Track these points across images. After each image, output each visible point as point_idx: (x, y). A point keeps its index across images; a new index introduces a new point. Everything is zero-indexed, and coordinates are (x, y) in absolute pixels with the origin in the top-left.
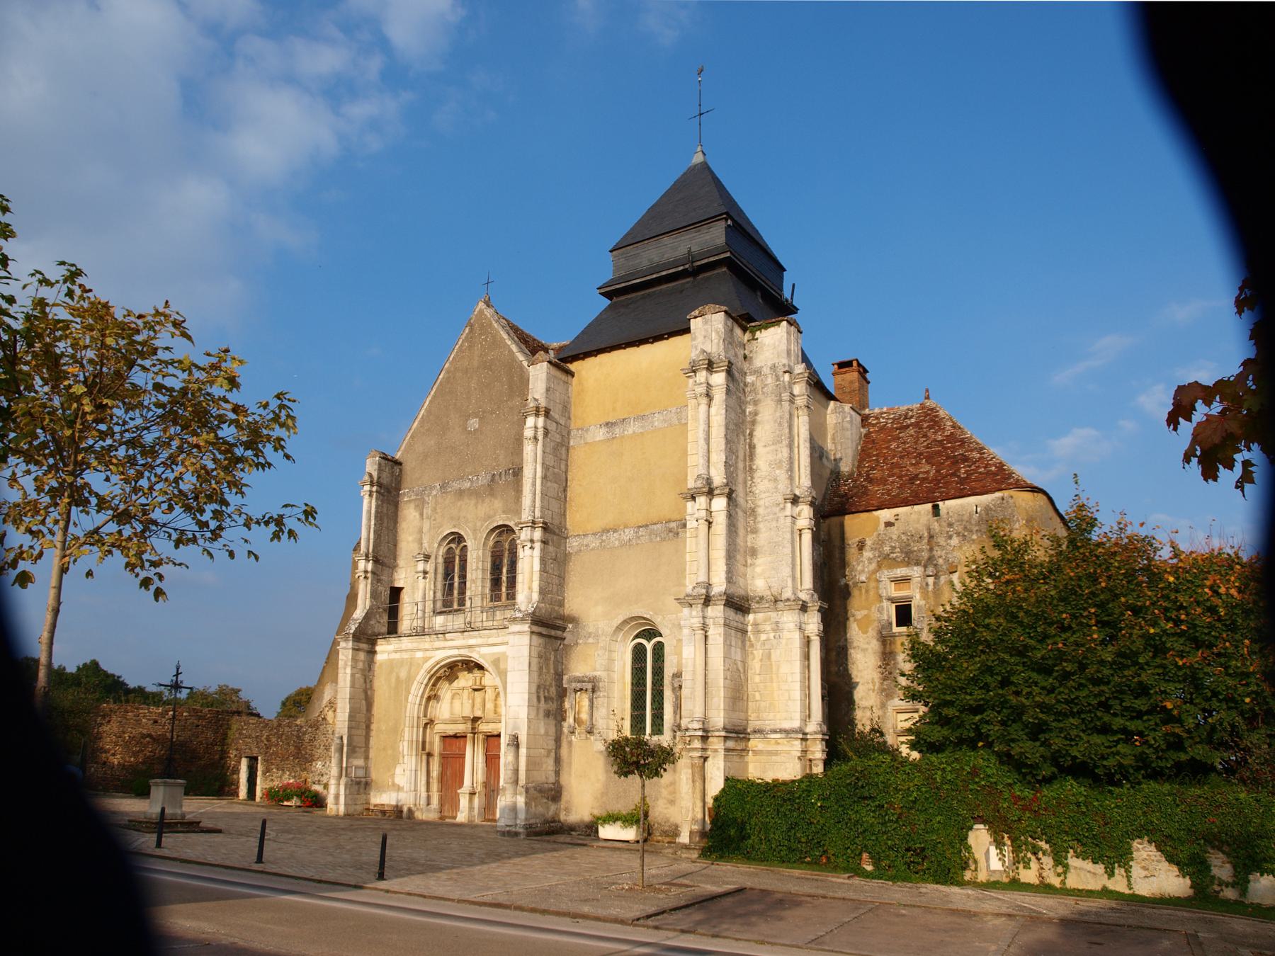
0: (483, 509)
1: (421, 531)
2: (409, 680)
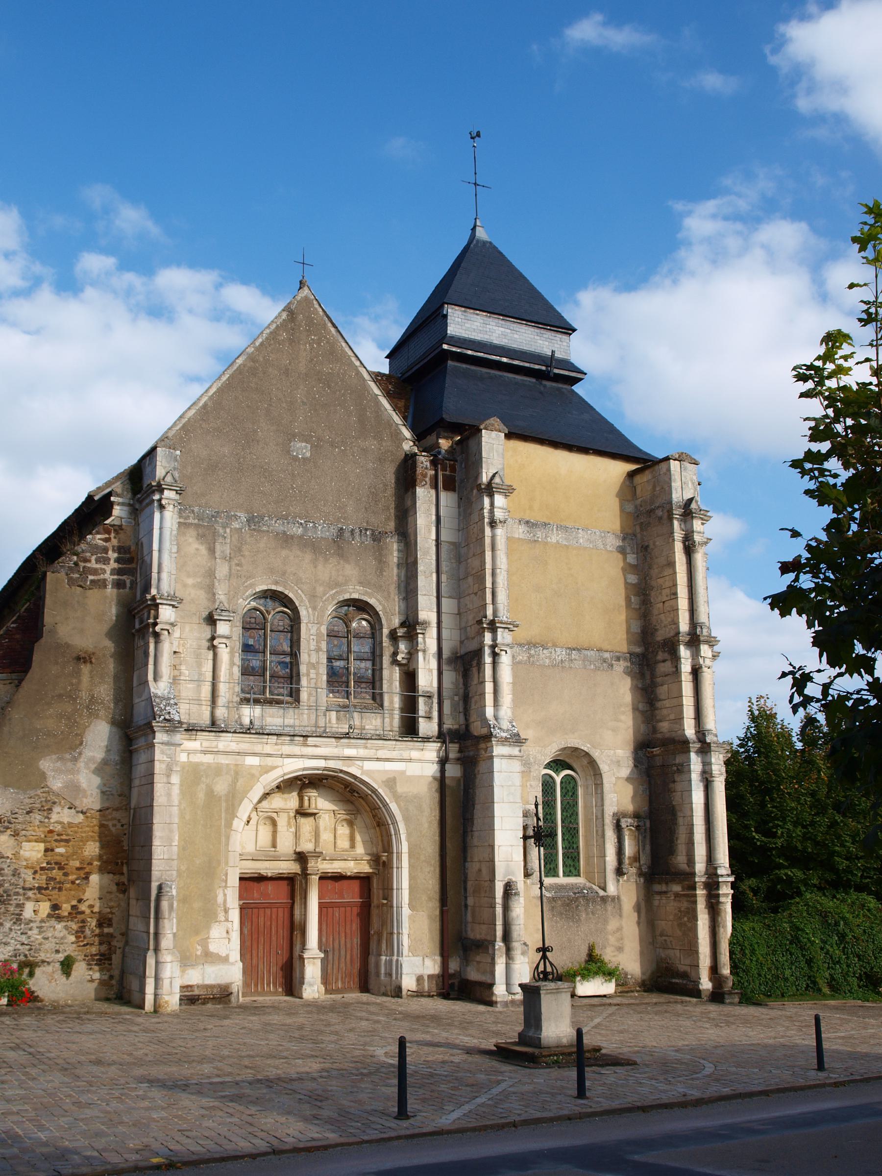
0: (327, 570)
1: (211, 574)
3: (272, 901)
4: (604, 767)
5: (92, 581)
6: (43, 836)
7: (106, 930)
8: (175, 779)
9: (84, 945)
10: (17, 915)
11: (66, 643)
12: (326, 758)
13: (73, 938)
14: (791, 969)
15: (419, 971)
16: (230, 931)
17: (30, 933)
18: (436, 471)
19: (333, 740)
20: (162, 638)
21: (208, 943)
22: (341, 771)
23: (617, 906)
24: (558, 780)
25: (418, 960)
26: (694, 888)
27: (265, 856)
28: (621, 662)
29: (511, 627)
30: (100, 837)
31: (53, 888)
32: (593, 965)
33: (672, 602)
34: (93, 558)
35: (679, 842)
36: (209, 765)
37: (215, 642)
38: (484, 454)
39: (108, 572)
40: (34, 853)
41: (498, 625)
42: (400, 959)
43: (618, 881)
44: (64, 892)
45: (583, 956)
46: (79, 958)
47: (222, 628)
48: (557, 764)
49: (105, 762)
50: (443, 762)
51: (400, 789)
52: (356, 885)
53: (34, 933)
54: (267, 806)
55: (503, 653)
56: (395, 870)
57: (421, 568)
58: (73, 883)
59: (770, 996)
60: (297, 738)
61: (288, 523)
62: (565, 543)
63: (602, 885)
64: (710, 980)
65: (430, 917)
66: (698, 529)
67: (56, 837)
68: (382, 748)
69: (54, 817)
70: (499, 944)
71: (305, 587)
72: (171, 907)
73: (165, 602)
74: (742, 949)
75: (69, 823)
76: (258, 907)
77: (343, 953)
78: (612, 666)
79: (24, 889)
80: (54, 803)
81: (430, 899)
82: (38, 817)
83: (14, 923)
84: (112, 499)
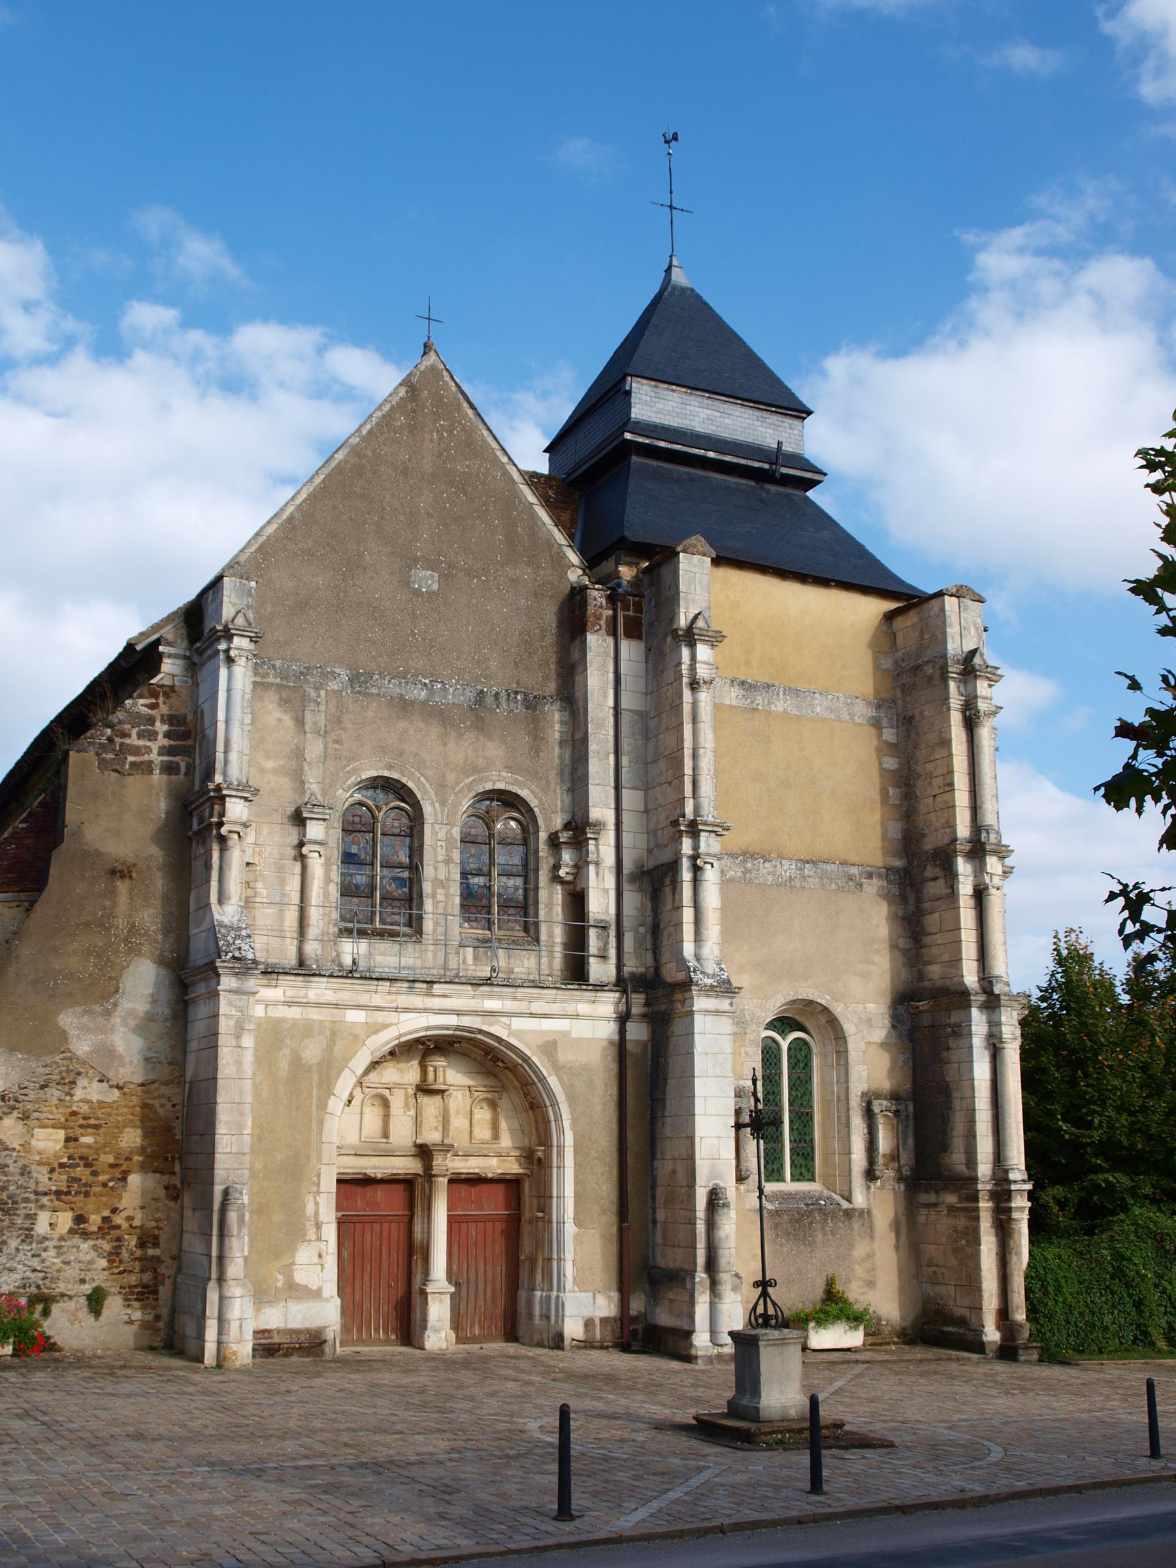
0: (461, 749)
1: (298, 754)
2: (329, 1070)
3: (381, 1212)
4: (849, 1028)
5: (133, 764)
6: (63, 1120)
7: (151, 1252)
8: (248, 1041)
9: (120, 1273)
10: (27, 1229)
11: (96, 850)
12: (458, 1013)
13: (104, 1263)
14: (1112, 1313)
15: (588, 1312)
16: (324, 1254)
17: (44, 1255)
18: (615, 611)
19: (469, 987)
20: (230, 843)
21: (292, 1271)
22: (480, 1031)
23: (866, 1223)
24: (785, 1045)
25: (586, 1297)
26: (975, 1198)
27: (373, 1150)
28: (875, 880)
29: (719, 830)
30: (142, 1121)
31: (78, 1193)
32: (833, 1305)
33: (946, 796)
34: (134, 732)
35: (955, 1133)
36: (295, 1023)
37: (305, 850)
38: (682, 588)
39: (155, 751)
40: (50, 1144)
41: (700, 827)
42: (562, 1295)
43: (869, 1188)
44: (92, 1198)
45: (819, 1293)
46: (113, 1290)
47: (315, 830)
48: (783, 1023)
49: (150, 1017)
50: (623, 1019)
51: (563, 1057)
52: (499, 1191)
53: (50, 1256)
54: (376, 1080)
55: (708, 866)
56: (555, 1170)
57: (593, 747)
58: (105, 1185)
59: (1083, 1351)
60: (418, 985)
61: (407, 683)
62: (795, 712)
63: (846, 1194)
64: (998, 1328)
65: (603, 1237)
66: (984, 694)
67: (81, 1122)
68: (538, 999)
69: (79, 1093)
70: (701, 1276)
71: (430, 773)
72: (241, 1220)
73: (234, 793)
74: (1042, 1285)
75: (100, 1102)
76: (362, 1221)
77: (481, 1286)
78: (861, 885)
79: (36, 1193)
80: (79, 1074)
81: (604, 1211)
82: (57, 1093)
83: (23, 1241)
84: (161, 648)
